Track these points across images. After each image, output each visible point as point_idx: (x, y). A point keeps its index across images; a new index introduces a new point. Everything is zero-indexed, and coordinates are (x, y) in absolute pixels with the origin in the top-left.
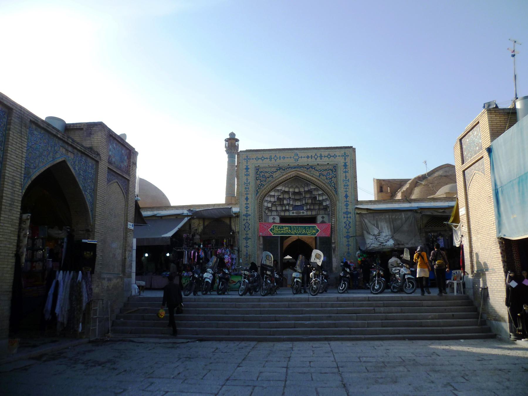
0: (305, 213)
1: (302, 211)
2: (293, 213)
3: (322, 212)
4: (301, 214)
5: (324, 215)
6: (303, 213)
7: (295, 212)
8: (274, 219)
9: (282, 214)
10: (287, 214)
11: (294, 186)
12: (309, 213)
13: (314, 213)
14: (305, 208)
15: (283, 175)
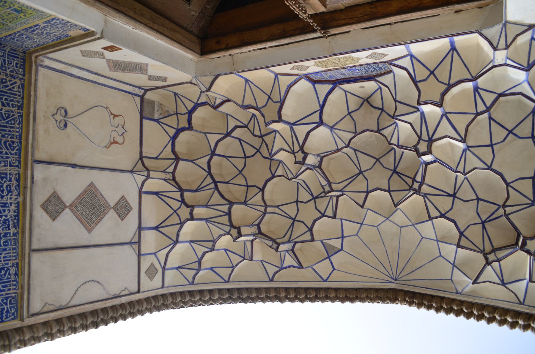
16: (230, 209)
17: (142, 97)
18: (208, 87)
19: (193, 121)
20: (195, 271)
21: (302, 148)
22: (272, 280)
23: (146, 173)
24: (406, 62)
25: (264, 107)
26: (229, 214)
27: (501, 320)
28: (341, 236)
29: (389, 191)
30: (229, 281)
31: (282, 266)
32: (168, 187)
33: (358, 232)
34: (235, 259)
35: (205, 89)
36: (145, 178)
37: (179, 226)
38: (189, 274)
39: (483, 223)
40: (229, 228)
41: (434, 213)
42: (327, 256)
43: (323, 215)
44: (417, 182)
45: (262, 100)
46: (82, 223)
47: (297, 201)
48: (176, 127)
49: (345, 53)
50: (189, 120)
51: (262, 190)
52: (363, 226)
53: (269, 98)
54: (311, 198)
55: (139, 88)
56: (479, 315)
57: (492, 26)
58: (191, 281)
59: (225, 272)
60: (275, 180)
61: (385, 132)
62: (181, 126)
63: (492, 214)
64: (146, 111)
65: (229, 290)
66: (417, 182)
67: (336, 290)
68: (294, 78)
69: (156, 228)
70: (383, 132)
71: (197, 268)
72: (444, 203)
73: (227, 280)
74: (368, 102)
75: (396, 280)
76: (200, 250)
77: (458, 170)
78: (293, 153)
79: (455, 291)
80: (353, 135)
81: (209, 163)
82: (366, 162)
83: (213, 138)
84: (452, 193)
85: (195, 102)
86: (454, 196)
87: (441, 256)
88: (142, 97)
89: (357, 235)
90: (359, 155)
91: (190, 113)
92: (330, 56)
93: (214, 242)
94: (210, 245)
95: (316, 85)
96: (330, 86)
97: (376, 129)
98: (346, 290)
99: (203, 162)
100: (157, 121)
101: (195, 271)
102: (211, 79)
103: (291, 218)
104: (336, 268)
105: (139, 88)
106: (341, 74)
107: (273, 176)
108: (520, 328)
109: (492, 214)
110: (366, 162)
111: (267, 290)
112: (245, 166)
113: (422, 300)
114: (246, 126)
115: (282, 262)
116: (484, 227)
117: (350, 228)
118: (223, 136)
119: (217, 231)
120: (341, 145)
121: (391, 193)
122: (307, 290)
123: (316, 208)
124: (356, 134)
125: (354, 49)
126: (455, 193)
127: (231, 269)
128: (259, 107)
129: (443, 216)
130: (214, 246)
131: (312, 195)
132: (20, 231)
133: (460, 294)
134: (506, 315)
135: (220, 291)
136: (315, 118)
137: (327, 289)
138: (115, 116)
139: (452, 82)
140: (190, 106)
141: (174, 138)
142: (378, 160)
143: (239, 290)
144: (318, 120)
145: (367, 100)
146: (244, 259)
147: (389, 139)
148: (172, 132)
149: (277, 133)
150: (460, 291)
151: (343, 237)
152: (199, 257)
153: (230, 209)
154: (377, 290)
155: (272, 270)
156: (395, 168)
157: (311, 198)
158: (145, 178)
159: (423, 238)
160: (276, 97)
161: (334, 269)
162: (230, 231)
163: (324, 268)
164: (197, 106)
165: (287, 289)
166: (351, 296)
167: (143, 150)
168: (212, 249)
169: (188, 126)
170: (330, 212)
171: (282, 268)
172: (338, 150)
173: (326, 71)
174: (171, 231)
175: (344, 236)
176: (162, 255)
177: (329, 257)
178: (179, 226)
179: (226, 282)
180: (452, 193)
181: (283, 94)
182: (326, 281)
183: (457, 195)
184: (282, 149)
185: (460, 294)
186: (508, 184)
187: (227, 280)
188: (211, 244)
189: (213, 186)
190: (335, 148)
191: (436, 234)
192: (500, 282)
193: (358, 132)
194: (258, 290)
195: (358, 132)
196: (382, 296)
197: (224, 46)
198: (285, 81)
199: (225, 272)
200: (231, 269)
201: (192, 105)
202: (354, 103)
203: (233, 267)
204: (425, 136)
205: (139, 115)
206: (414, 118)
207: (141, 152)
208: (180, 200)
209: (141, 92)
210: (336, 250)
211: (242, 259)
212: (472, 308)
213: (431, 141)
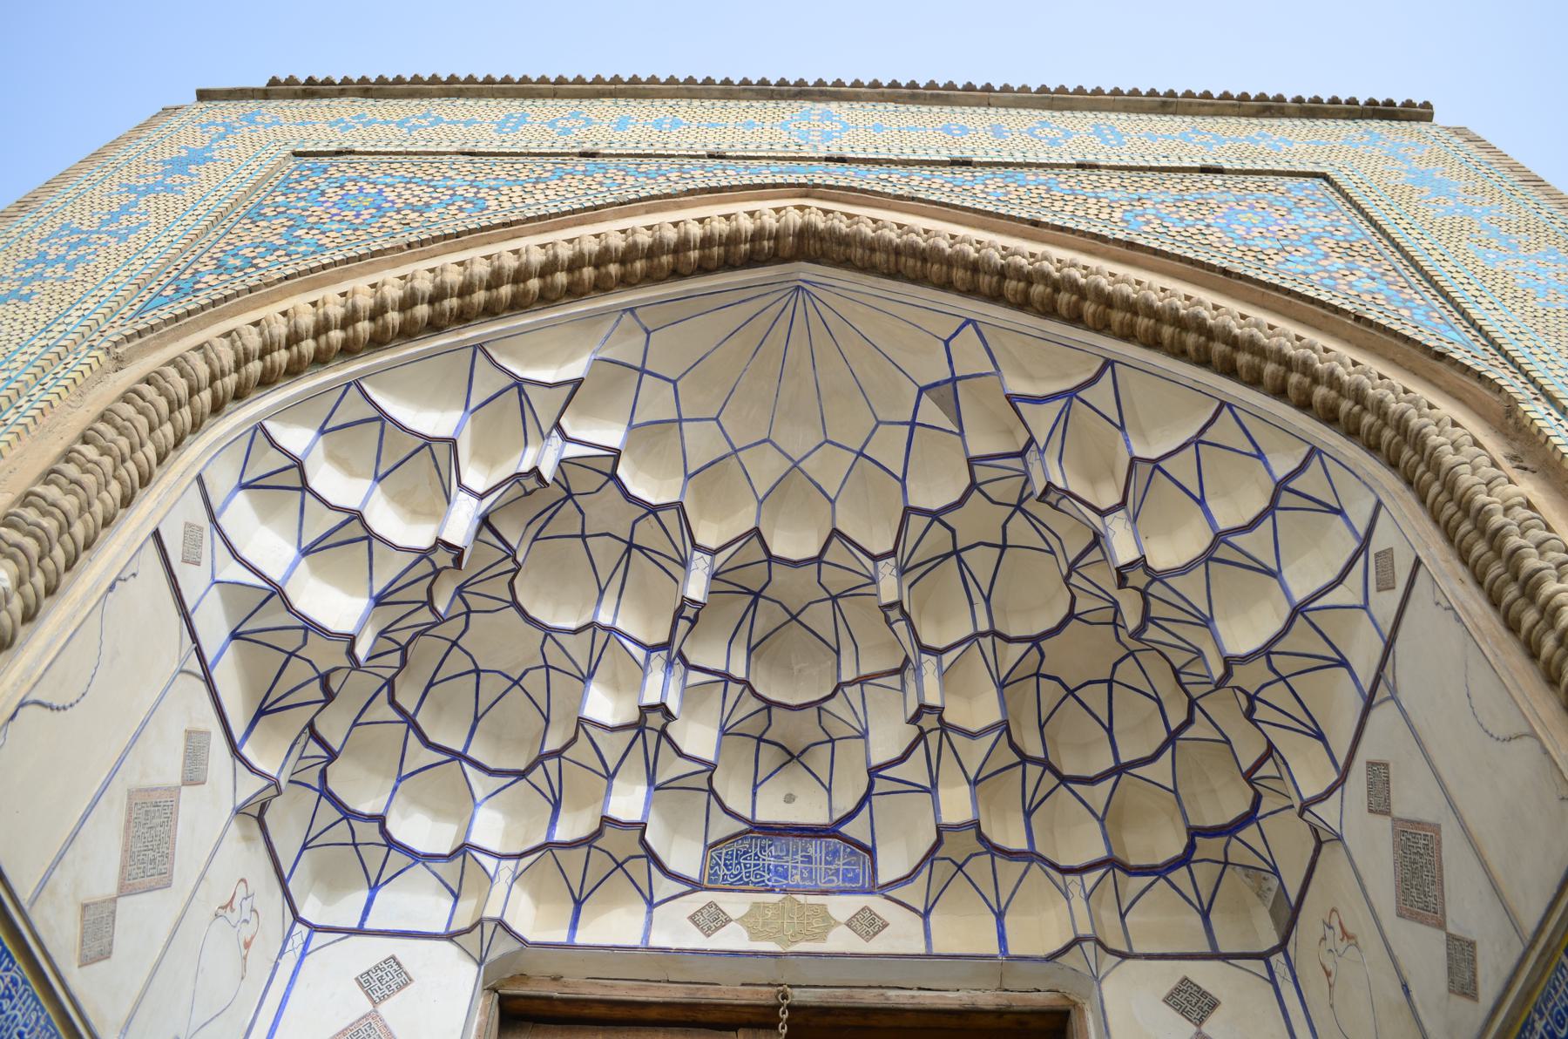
0: (901, 934)
1: (843, 907)
2: (712, 920)
3: (1161, 917)
4: (841, 941)
5: (1206, 975)
6: (869, 924)
7: (735, 904)
8: (383, 981)
9: (534, 918)
10: (615, 924)
11: (766, 468)
12: (963, 930)
13: (1041, 925)
14: (891, 865)
15: (624, 206)
16: (1142, 628)
17: (1282, 947)
18: (1077, 948)
19: (1185, 840)
20: (1291, 485)
21: (922, 736)
22: (1109, 363)
23: (1307, 815)
24: (664, 887)
25: (1121, 660)
26: (1147, 618)
27: (524, 281)
28: (917, 428)
29: (771, 558)
30: (1222, 404)
31: (1069, 403)
32: (1280, 739)
33: (873, 431)
34: (1182, 468)
35: (1085, 945)
36: (1313, 808)
37: (1274, 649)
38: (1310, 483)
39: (570, 495)
40: (1150, 590)
41: (669, 518)
42: (959, 384)
43: (935, 515)
44: (687, 618)
45: (980, 867)
46: (1441, 869)
47: (1003, 547)
48: (1234, 841)
49: (755, 954)
50: (1191, 847)
51: (1071, 615)
52: (857, 448)
53: (960, 868)
54: (963, 555)
55: (1273, 981)
56: (580, 268)
57: (503, 957)
58: (1317, 458)
59: (1225, 430)
60: (1037, 629)
61: (755, 704)
62: (1222, 840)
63: (551, 517)
64: (1288, 916)
65: (1229, 370)
66: (687, 618)
67: (947, 285)
68: (892, 893)
69: (1343, 663)
70: (759, 705)
71: (1284, 493)
72: (647, 533)
73: (1226, 409)
74: (789, 753)
75: (798, 288)
76: (1257, 544)
77: (606, 634)
78: (944, 727)
79: (637, 312)
80: (826, 705)
81: (1189, 721)
82: (820, 617)
83: (1160, 771)
84: (634, 551)
85: (1162, 881)
86: (631, 546)
87: (674, 382)
88: (1282, 947)
89: (879, 423)
90: (832, 641)
91: (1185, 860)
92: (786, 954)
93: (1207, 557)
94: (1223, 552)
95: (869, 844)
96: (843, 829)
97: (774, 710)
98: (920, 280)
99: (1200, 729)
100: (1276, 872)
101: (1291, 485)
102: (1065, 960)
103: (1024, 512)
104: (942, 345)
105: (1273, 981)
106: (809, 859)
107: (1035, 641)
108: (481, 280)
109: (551, 517)
110: (820, 617)
111: (1128, 335)
112: (1115, 665)
113: (727, 252)
114: (1064, 780)
115: (1065, 417)
116: (568, 490)
117: (888, 447)
118: (1135, 771)
119: (1191, 587)
120: (853, 692)
121: (764, 557)
122: (1023, 304)
123: (953, 531)
124: (818, 704)
125: (735, 959)
126: (628, 551)
127: (1205, 437)
128: (988, 856)
129: (653, 510)
130: (1214, 545)
131: (960, 561)
132: (1530, 1007)
133: (625, 311)
134: (514, 296)
135: (1254, 381)
136: (880, 786)
137: (972, 292)
138: (1328, 974)
139: (584, 850)
140: (1180, 876)
141: (1249, 818)
142: (794, 617)
143: (1204, 361)
144: (877, 780)
145: (793, 757)
146: (1156, 463)
147: (747, 692)
148: (1249, 834)
149: (972, 777)
150: (627, 317)
151: (913, 424)
152: (1269, 519)
153: (1142, 628)
154: (846, 263)
155: (1101, 395)
156: (755, 603)
157: (963, 555)
158: (1313, 808)
159: (716, 419)
160: (942, 869)
161: (947, 343)
162: (1151, 583)
163: (971, 357)
164: (1160, 871)
165: (1076, 319)
166: (911, 262)
167: (1310, 853)
168: (1220, 537)
169: (1197, 839)
170: (917, 523)
171: (1070, 394)
172: (862, 680)
173: (825, 892)
174: (1303, 638)
175: (907, 428)
176: (1347, 594)
177: (954, 380)
178: (1274, 649)
179: (1230, 406)
180: (634, 551)
181: (926, 871)
182: (968, 321)
183: (625, 546)
184: (973, 735)
185: (625, 311)
186: (515, 604)
187: (1226, 409)
188: (1218, 554)
189: (1184, 678)
190: (866, 687)
191: (682, 438)
192: (526, 387)
193: (814, 710)
194: (1154, 343)
195: (814, 710)
196: (835, 248)
197: (1008, 1017)
198: (914, 894)
199: (1225, 430)
200: (1205, 437)
201: (1172, 876)
202: (819, 759)
203: (1197, 441)
204: (652, 737)
205: (1300, 921)
206: (671, 769)
207: (1317, 851)
208: (1257, 703)
209: (1277, 960)
210: (934, 391)
211: (1162, 464)
212: (597, 278)
213: (639, 726)
